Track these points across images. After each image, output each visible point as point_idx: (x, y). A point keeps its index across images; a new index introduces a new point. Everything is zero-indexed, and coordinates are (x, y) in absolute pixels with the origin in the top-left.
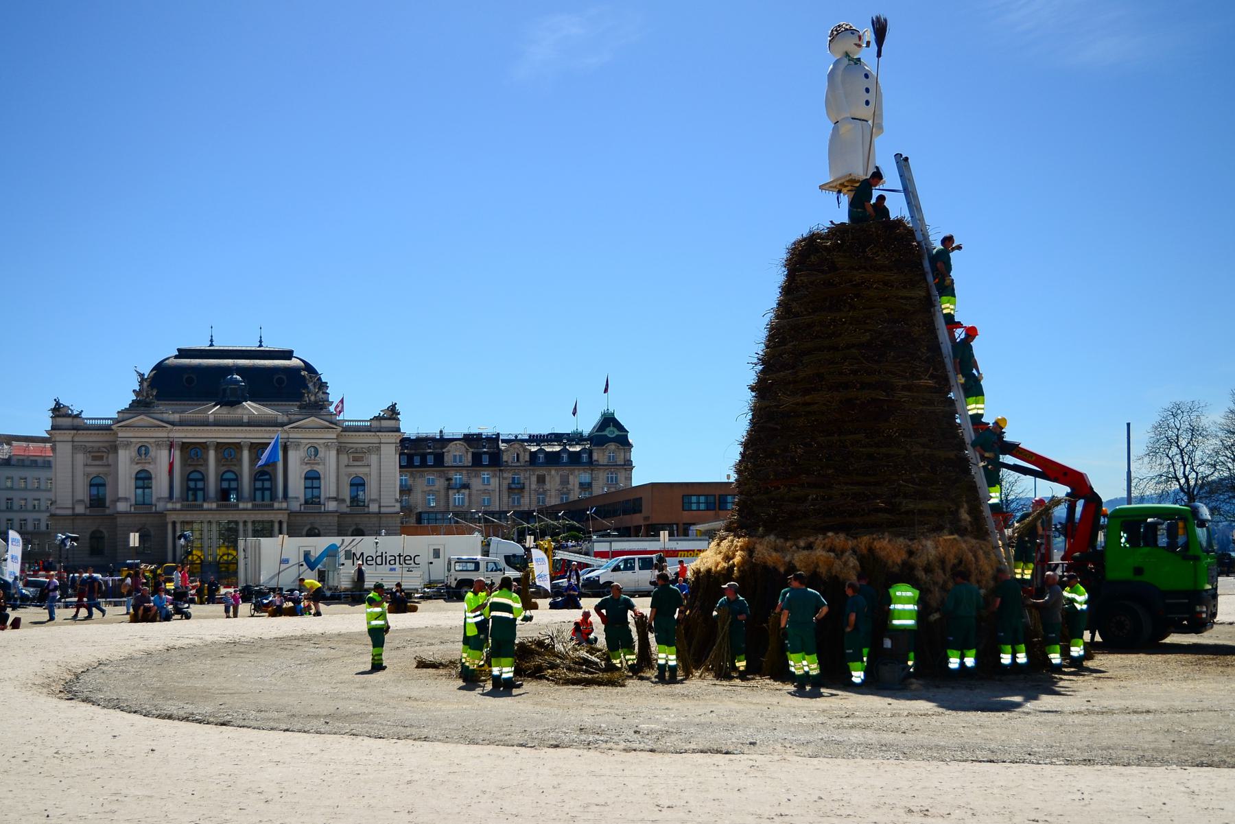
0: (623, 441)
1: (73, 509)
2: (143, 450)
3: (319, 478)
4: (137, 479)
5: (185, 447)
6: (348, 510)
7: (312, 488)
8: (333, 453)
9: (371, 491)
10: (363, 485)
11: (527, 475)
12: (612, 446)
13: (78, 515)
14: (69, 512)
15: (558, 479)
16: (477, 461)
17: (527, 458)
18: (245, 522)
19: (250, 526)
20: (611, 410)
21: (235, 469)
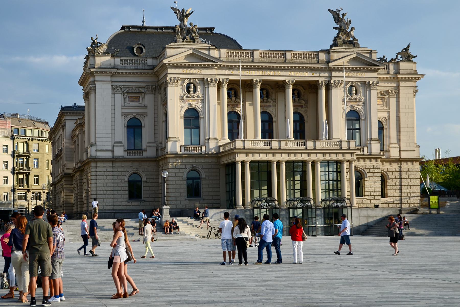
13: (118, 158)
14: (109, 154)
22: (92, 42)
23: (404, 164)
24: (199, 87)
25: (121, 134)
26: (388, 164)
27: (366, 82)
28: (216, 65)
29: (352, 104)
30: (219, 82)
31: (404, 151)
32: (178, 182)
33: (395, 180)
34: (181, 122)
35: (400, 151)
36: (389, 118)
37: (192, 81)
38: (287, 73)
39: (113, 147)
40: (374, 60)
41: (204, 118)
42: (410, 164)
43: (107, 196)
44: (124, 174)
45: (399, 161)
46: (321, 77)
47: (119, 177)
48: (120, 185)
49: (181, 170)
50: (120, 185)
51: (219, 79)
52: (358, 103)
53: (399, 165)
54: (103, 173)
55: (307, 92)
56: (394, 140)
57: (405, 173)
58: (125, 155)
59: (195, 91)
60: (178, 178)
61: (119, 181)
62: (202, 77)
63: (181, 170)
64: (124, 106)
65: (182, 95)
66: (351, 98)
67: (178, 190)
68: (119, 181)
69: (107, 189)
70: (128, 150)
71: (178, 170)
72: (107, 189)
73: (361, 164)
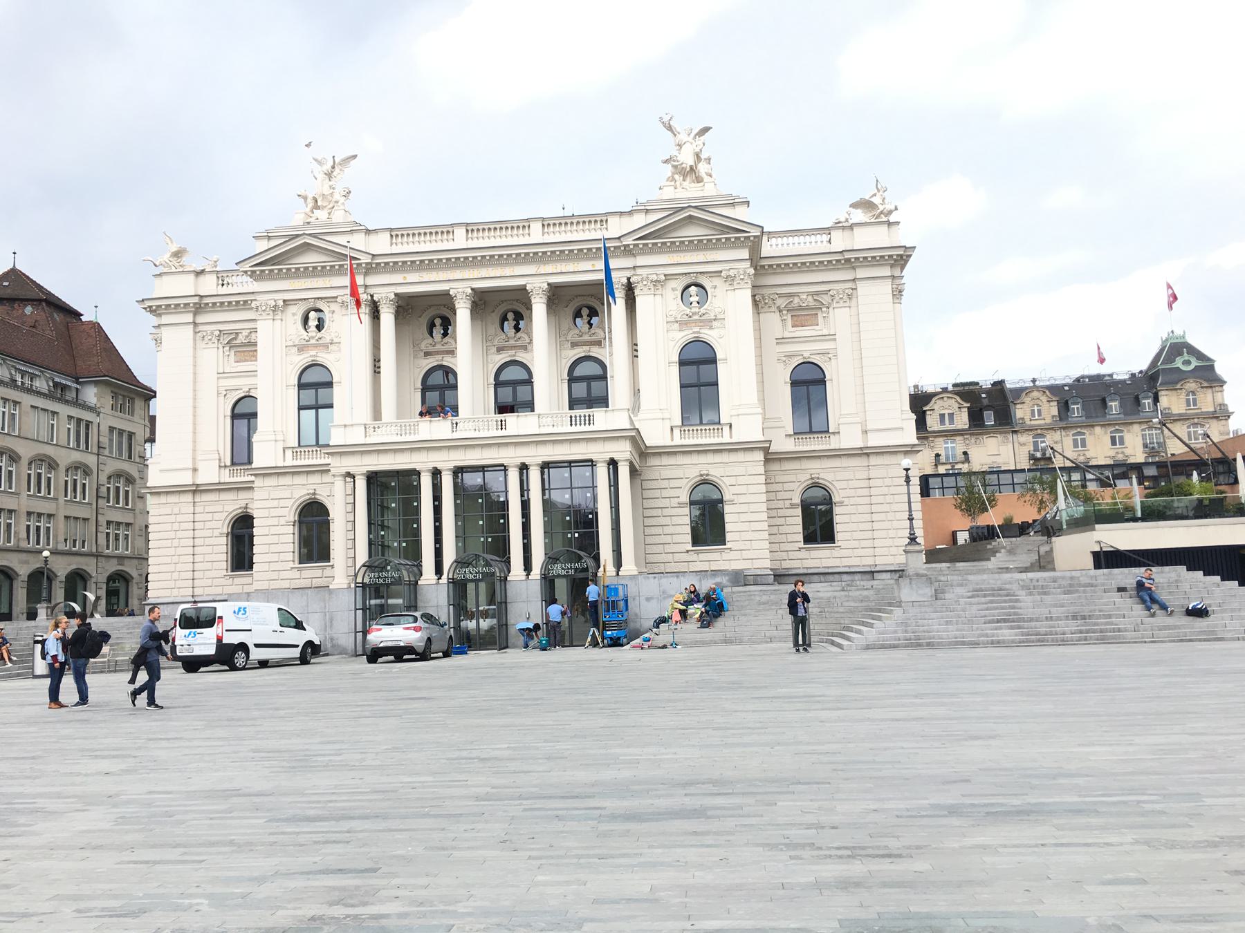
0: (1207, 375)
1: (195, 470)
2: (314, 318)
3: (714, 361)
4: (301, 386)
5: (407, 307)
6: (789, 445)
8: (745, 295)
10: (822, 382)
11: (1057, 435)
12: (1191, 385)
14: (186, 479)
15: (1107, 440)
16: (976, 419)
17: (1055, 411)
18: (524, 468)
19: (534, 476)
20: (1178, 332)
21: (521, 356)
25: (217, 435)
32: (274, 530)
33: (852, 501)
34: (292, 396)
38: (531, 269)
39: (194, 459)
43: (179, 567)
44: (217, 517)
47: (208, 525)
48: (208, 541)
49: (283, 503)
50: (208, 541)
54: (172, 519)
55: (581, 305)
58: (226, 477)
59: (319, 328)
60: (275, 521)
61: (209, 533)
63: (283, 503)
64: (222, 374)
67: (274, 548)
68: (209, 533)
69: (180, 551)
70: (233, 464)
71: (275, 503)
72: (180, 551)
73: (716, 468)
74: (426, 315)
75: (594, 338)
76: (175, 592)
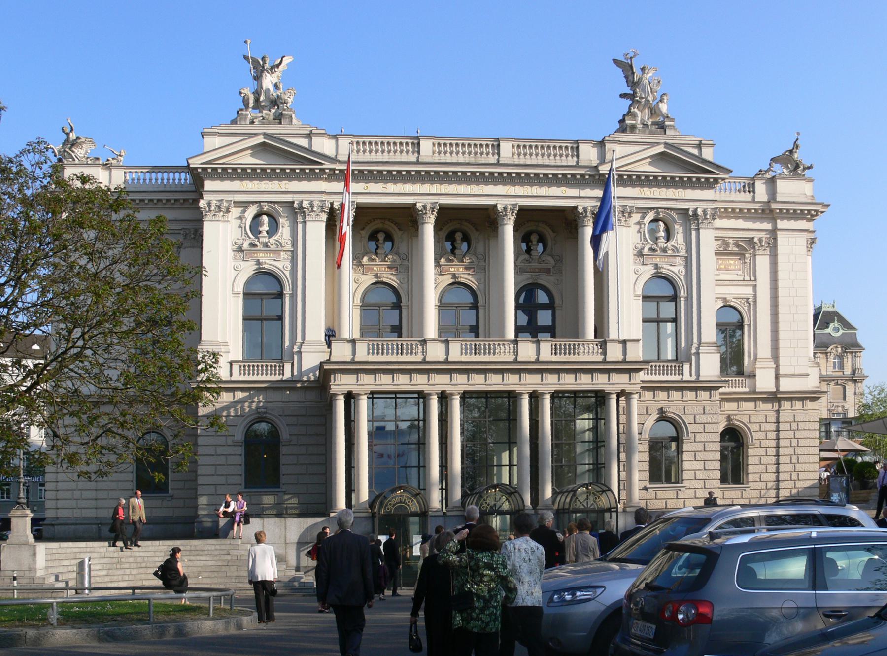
3: (674, 298)
4: (247, 295)
7: (658, 321)
9: (757, 344)
22: (65, 137)
23: (786, 405)
24: (282, 221)
26: (751, 405)
27: (688, 210)
28: (322, 170)
29: (657, 260)
30: (332, 209)
31: (786, 375)
35: (777, 376)
36: (755, 302)
37: (265, 209)
40: (705, 161)
41: (293, 296)
42: (798, 404)
45: (775, 397)
46: (585, 199)
51: (332, 204)
52: (672, 260)
53: (776, 408)
55: (550, 233)
56: (764, 351)
57: (787, 426)
59: (272, 232)
62: (288, 198)
65: (240, 242)
66: (655, 247)
74: (384, 229)
75: (543, 265)
76: (77, 513)
